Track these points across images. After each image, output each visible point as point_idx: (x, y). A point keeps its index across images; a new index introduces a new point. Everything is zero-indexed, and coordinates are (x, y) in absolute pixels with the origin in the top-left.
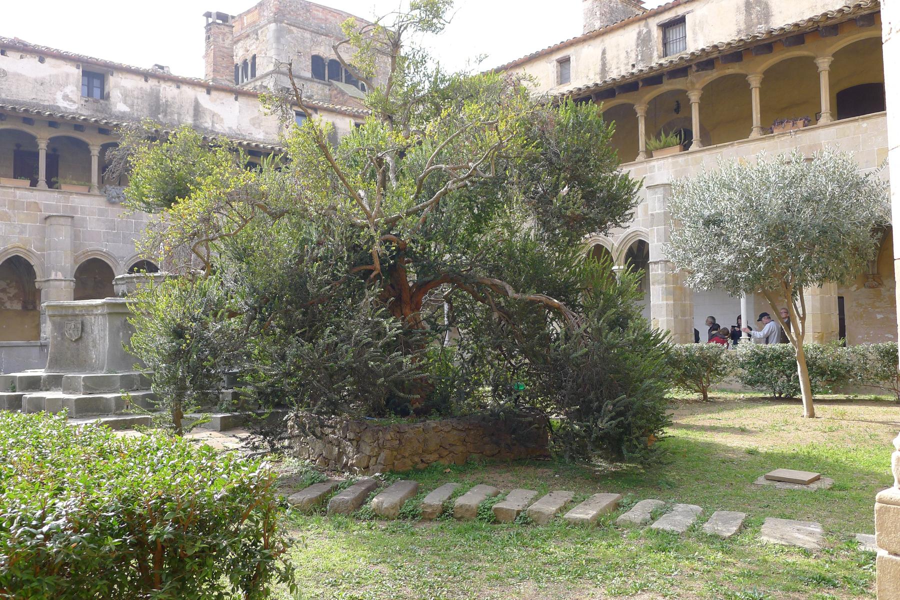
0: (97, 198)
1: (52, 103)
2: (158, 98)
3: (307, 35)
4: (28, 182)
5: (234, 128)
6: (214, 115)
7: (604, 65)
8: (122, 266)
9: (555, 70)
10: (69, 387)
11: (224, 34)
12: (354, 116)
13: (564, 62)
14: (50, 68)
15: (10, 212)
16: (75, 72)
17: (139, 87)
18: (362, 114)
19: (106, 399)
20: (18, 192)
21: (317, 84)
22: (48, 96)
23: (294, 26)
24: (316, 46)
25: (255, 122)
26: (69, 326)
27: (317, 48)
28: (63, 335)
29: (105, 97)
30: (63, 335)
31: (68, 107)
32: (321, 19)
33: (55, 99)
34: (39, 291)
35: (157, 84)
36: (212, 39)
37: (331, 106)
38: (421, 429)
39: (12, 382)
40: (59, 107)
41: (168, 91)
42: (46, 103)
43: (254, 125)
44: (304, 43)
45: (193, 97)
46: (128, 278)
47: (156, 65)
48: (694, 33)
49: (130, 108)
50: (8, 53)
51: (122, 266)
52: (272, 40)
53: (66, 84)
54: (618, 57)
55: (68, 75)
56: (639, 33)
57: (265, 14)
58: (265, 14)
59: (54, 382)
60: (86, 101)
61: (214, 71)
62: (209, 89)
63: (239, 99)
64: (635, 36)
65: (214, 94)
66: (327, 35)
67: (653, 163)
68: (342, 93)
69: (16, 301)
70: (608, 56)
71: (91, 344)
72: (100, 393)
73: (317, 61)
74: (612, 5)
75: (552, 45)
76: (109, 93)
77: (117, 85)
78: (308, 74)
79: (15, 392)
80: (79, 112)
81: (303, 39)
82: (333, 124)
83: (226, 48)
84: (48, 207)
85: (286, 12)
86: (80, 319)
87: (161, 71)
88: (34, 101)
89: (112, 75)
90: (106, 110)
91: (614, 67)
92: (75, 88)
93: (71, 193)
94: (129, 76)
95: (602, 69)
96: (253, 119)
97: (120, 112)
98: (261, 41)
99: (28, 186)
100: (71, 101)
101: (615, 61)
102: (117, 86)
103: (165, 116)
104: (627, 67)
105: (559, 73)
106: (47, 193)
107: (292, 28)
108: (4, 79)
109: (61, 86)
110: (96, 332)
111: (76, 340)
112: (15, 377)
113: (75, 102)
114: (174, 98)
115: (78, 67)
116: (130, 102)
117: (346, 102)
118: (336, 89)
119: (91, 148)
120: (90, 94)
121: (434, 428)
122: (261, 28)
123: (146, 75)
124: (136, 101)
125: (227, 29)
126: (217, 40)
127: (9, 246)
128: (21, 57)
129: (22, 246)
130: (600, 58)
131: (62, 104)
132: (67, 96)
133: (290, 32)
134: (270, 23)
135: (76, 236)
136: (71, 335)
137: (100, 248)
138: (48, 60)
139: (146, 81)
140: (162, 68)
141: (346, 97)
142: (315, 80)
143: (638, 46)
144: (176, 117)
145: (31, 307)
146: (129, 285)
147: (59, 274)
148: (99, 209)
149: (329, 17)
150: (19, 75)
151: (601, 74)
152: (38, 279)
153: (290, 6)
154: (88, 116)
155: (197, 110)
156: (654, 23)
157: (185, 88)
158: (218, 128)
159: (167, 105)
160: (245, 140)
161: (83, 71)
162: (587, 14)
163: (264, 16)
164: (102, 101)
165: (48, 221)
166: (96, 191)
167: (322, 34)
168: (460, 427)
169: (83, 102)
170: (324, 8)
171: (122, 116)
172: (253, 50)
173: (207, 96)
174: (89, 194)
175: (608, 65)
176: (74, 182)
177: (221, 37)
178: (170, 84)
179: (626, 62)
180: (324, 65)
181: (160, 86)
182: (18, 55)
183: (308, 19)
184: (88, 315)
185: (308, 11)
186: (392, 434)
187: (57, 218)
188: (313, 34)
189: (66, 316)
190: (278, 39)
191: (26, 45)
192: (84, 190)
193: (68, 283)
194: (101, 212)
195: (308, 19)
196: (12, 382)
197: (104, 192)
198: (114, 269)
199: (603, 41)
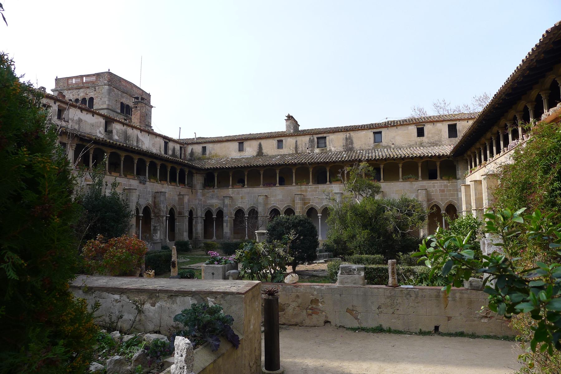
0: (136, 181)
1: (95, 134)
3: (120, 93)
6: (142, 142)
21: (122, 116)
24: (122, 98)
25: (154, 145)
48: (329, 143)
54: (302, 144)
56: (310, 138)
61: (140, 122)
62: (141, 131)
63: (142, 132)
64: (309, 139)
66: (126, 94)
67: (332, 185)
70: (298, 143)
78: (119, 111)
81: (118, 94)
90: (111, 138)
94: (119, 124)
102: (115, 128)
107: (114, 89)
114: (131, 134)
116: (118, 135)
122: (99, 86)
131: (99, 135)
134: (105, 85)
143: (309, 142)
155: (138, 140)
156: (315, 137)
157: (134, 130)
167: (125, 93)
171: (117, 141)
172: (92, 94)
178: (130, 128)
182: (86, 112)
185: (120, 81)
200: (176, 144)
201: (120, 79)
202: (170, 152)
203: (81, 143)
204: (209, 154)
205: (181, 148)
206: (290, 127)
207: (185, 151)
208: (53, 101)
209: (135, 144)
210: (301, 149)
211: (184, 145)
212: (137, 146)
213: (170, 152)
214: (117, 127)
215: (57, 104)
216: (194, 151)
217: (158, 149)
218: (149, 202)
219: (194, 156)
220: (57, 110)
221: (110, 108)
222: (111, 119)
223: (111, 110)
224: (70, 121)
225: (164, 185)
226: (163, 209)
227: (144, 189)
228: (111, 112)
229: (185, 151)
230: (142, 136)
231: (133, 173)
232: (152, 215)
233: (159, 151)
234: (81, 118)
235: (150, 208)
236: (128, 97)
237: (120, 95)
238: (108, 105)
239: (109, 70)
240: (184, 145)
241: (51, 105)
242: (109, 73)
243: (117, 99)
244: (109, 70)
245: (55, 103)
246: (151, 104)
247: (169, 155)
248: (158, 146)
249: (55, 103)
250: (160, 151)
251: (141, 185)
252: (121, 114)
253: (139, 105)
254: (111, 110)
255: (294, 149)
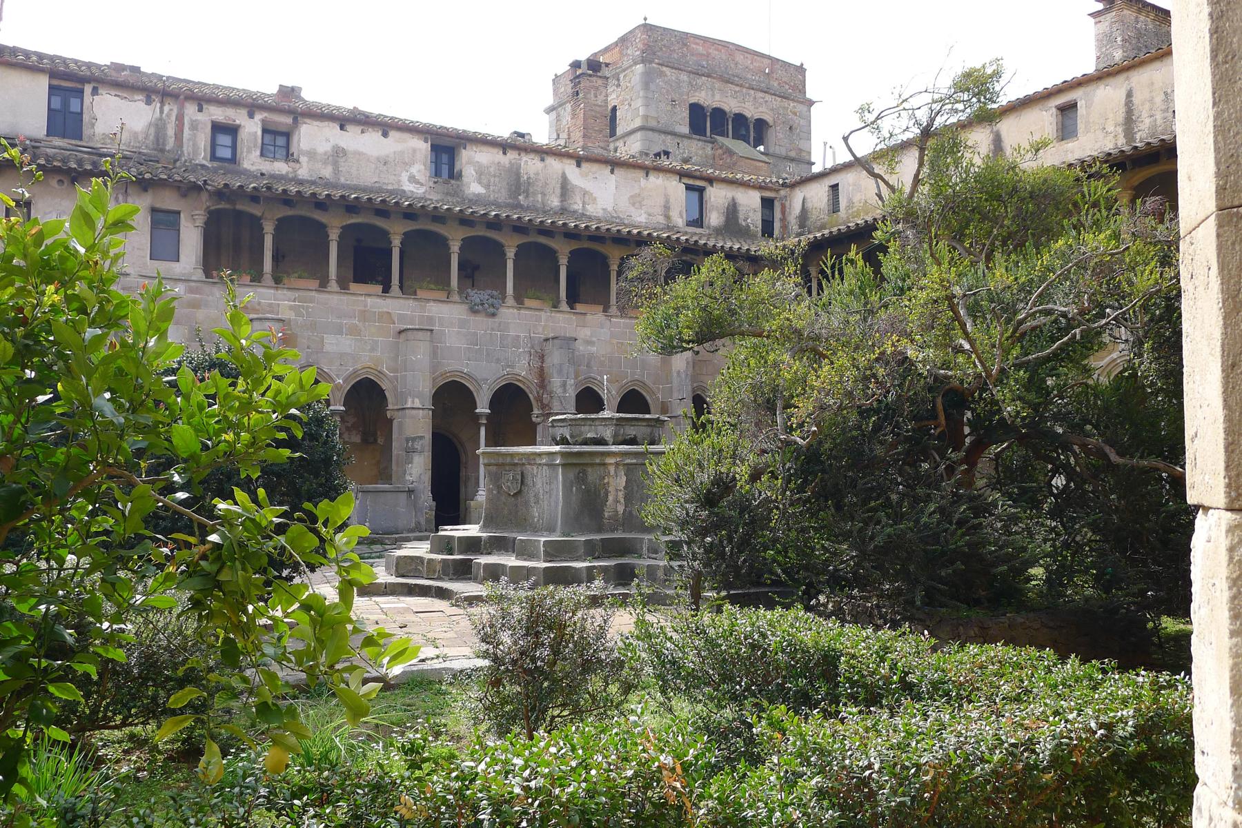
1: (396, 187)
2: (518, 175)
3: (684, 77)
4: (379, 288)
5: (610, 209)
6: (585, 193)
7: (1129, 112)
8: (485, 390)
9: (1053, 120)
10: (524, 551)
11: (597, 88)
12: (760, 188)
13: (1068, 109)
14: (394, 144)
15: (360, 325)
16: (422, 147)
17: (496, 161)
18: (770, 185)
19: (575, 568)
20: (369, 300)
21: (696, 142)
22: (392, 178)
23: (667, 66)
24: (695, 91)
25: (636, 201)
26: (506, 478)
27: (697, 94)
28: (499, 488)
29: (454, 175)
30: (499, 488)
31: (415, 190)
32: (702, 55)
33: (400, 181)
34: (391, 421)
35: (517, 157)
36: (581, 95)
37: (731, 176)
38: (1006, 625)
39: (448, 543)
40: (404, 191)
41: (531, 165)
42: (390, 187)
43: (634, 204)
44: (679, 87)
45: (560, 172)
46: (571, 420)
47: (515, 133)
49: (486, 189)
50: (348, 127)
51: (485, 390)
52: (638, 87)
53: (412, 163)
54: (1151, 100)
55: (414, 151)
57: (629, 52)
58: (629, 52)
59: (500, 545)
60: (435, 183)
61: (584, 136)
63: (616, 171)
65: (585, 166)
66: (709, 76)
68: (730, 153)
69: (354, 432)
70: (1137, 100)
71: (532, 499)
72: (561, 561)
73: (696, 111)
74: (1138, 26)
75: (1049, 86)
76: (461, 171)
77: (472, 161)
78: (686, 130)
79: (451, 554)
80: (427, 196)
81: (679, 82)
82: (733, 199)
83: (600, 106)
84: (402, 318)
85: (657, 49)
86: (519, 469)
87: (522, 140)
88: (377, 185)
89: (465, 148)
90: (457, 193)
91: (1145, 114)
92: (423, 167)
93: (429, 300)
94: (485, 148)
95: (1126, 119)
96: (631, 196)
97: (474, 194)
98: (624, 87)
99: (380, 294)
100: (418, 182)
101: (1147, 106)
103: (527, 197)
104: (1166, 114)
105: (1060, 124)
106: (402, 301)
107: (664, 69)
108: (344, 159)
109: (407, 165)
110: (539, 485)
111: (515, 494)
112: (452, 537)
113: (422, 185)
114: (537, 174)
115: (426, 141)
117: (735, 164)
118: (721, 148)
119: (451, 243)
120: (437, 173)
121: (1022, 624)
122: (624, 70)
123: (504, 146)
124: (492, 180)
125: (600, 82)
126: (588, 96)
127: (359, 366)
128: (363, 132)
129: (373, 366)
130: (1123, 101)
131: (408, 187)
132: (414, 177)
133: (662, 74)
134: (636, 64)
135: (434, 353)
136: (509, 487)
137: (459, 368)
138: (393, 134)
139: (505, 153)
140: (522, 135)
141: (735, 158)
142: (694, 136)
144: (539, 197)
145: (372, 440)
146: (573, 428)
147: (417, 400)
148: (459, 319)
149: (711, 51)
150: (360, 154)
151: (1126, 124)
152: (390, 407)
153: (662, 40)
154: (437, 201)
155: (565, 188)
158: (591, 210)
159: (529, 183)
160: (636, 227)
161: (432, 145)
162: (1102, 41)
163: (627, 55)
164: (453, 182)
165: (403, 335)
166: (456, 297)
167: (703, 75)
168: (1051, 624)
169: (431, 184)
170: (706, 40)
171: (477, 200)
173: (577, 170)
174: (447, 301)
175: (1135, 112)
176: (433, 286)
177: (593, 92)
178: (532, 156)
179: (1163, 107)
180: (705, 116)
181: (520, 160)
182: (359, 129)
183: (684, 56)
184: (530, 464)
185: (685, 45)
186: (976, 629)
187: (415, 332)
188: (692, 76)
189: (503, 464)
190: (646, 85)
191: (367, 117)
192: (442, 295)
193: (426, 411)
194: (462, 324)
195: (684, 56)
196: (448, 543)
197: (465, 298)
198: (475, 394)
199: (1128, 79)
200: (741, 189)
201: (684, 39)
202: (714, 219)
203: (223, 205)
204: (848, 208)
205: (767, 204)
206: (1109, 41)
207: (783, 212)
208: (244, 112)
209: (555, 202)
210: (1147, 121)
211: (777, 191)
212: (563, 211)
213: (714, 219)
214: (476, 159)
215: (259, 117)
216: (809, 205)
217: (658, 210)
218: (517, 371)
219: (808, 223)
220: (260, 133)
221: (653, 124)
222: (449, 136)
223: (652, 130)
224: (303, 159)
225: (589, 317)
226: (559, 391)
227: (493, 329)
228: (656, 135)
229: (783, 212)
230: (584, 175)
231: (448, 283)
232: (536, 411)
233: (661, 219)
234: (343, 144)
235: (527, 391)
236: (718, 85)
237: (685, 85)
238: (646, 117)
239: (645, 19)
240: (777, 191)
241: (238, 122)
242: (647, 28)
243: (676, 97)
244: (645, 19)
245: (251, 116)
246: (808, 95)
247: (709, 228)
248: (661, 201)
249: (251, 116)
250: (667, 217)
251: (480, 319)
252: (692, 138)
253: (584, 83)
254: (652, 130)
255: (1120, 129)
